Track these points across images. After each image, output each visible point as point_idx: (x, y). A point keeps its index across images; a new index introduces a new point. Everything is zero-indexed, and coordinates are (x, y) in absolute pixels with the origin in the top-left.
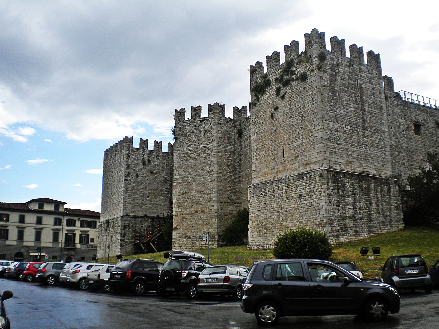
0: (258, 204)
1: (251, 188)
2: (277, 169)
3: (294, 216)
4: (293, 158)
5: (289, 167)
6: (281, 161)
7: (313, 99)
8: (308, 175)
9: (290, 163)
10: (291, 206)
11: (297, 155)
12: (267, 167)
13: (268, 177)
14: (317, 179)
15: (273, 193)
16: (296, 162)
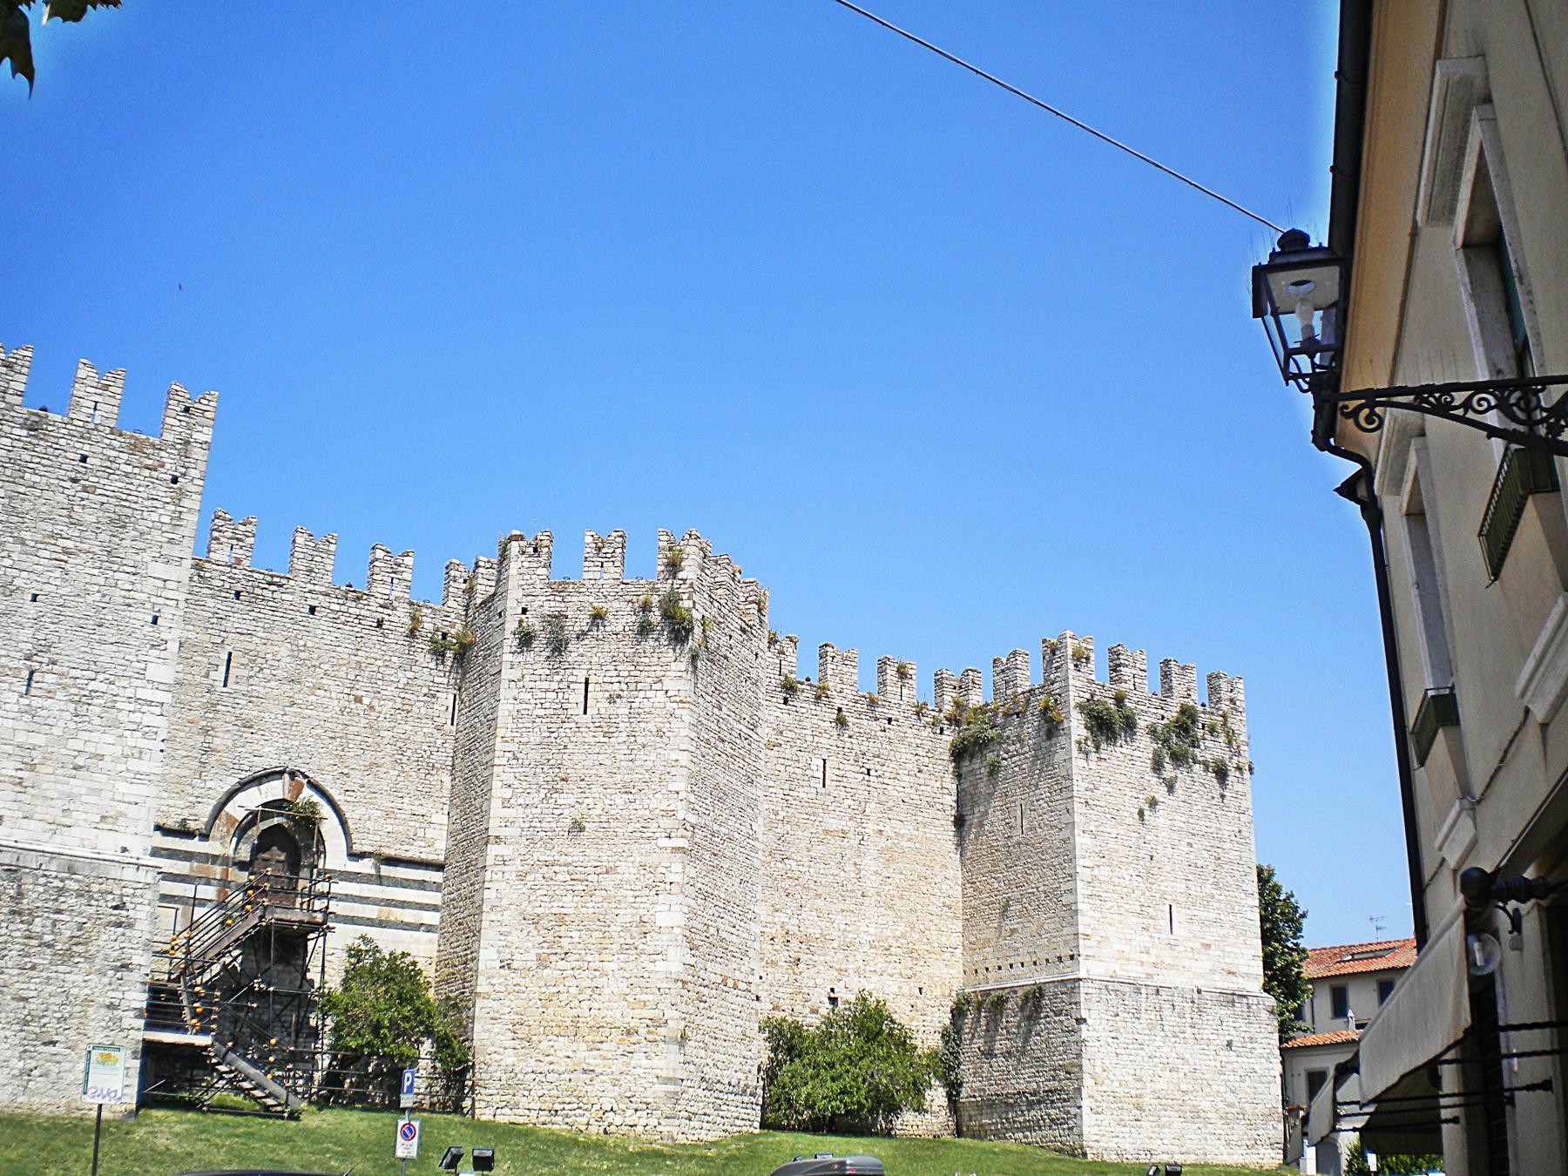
0: (1114, 1035)
1: (1090, 984)
2: (1157, 957)
3: (1215, 1088)
4: (1198, 946)
5: (1187, 963)
6: (1167, 942)
7: (1240, 831)
8: (1245, 1000)
9: (1190, 955)
10: (1207, 1063)
11: (1207, 942)
12: (1126, 939)
13: (1129, 967)
14: (1265, 1015)
15: (1158, 1018)
16: (1204, 957)
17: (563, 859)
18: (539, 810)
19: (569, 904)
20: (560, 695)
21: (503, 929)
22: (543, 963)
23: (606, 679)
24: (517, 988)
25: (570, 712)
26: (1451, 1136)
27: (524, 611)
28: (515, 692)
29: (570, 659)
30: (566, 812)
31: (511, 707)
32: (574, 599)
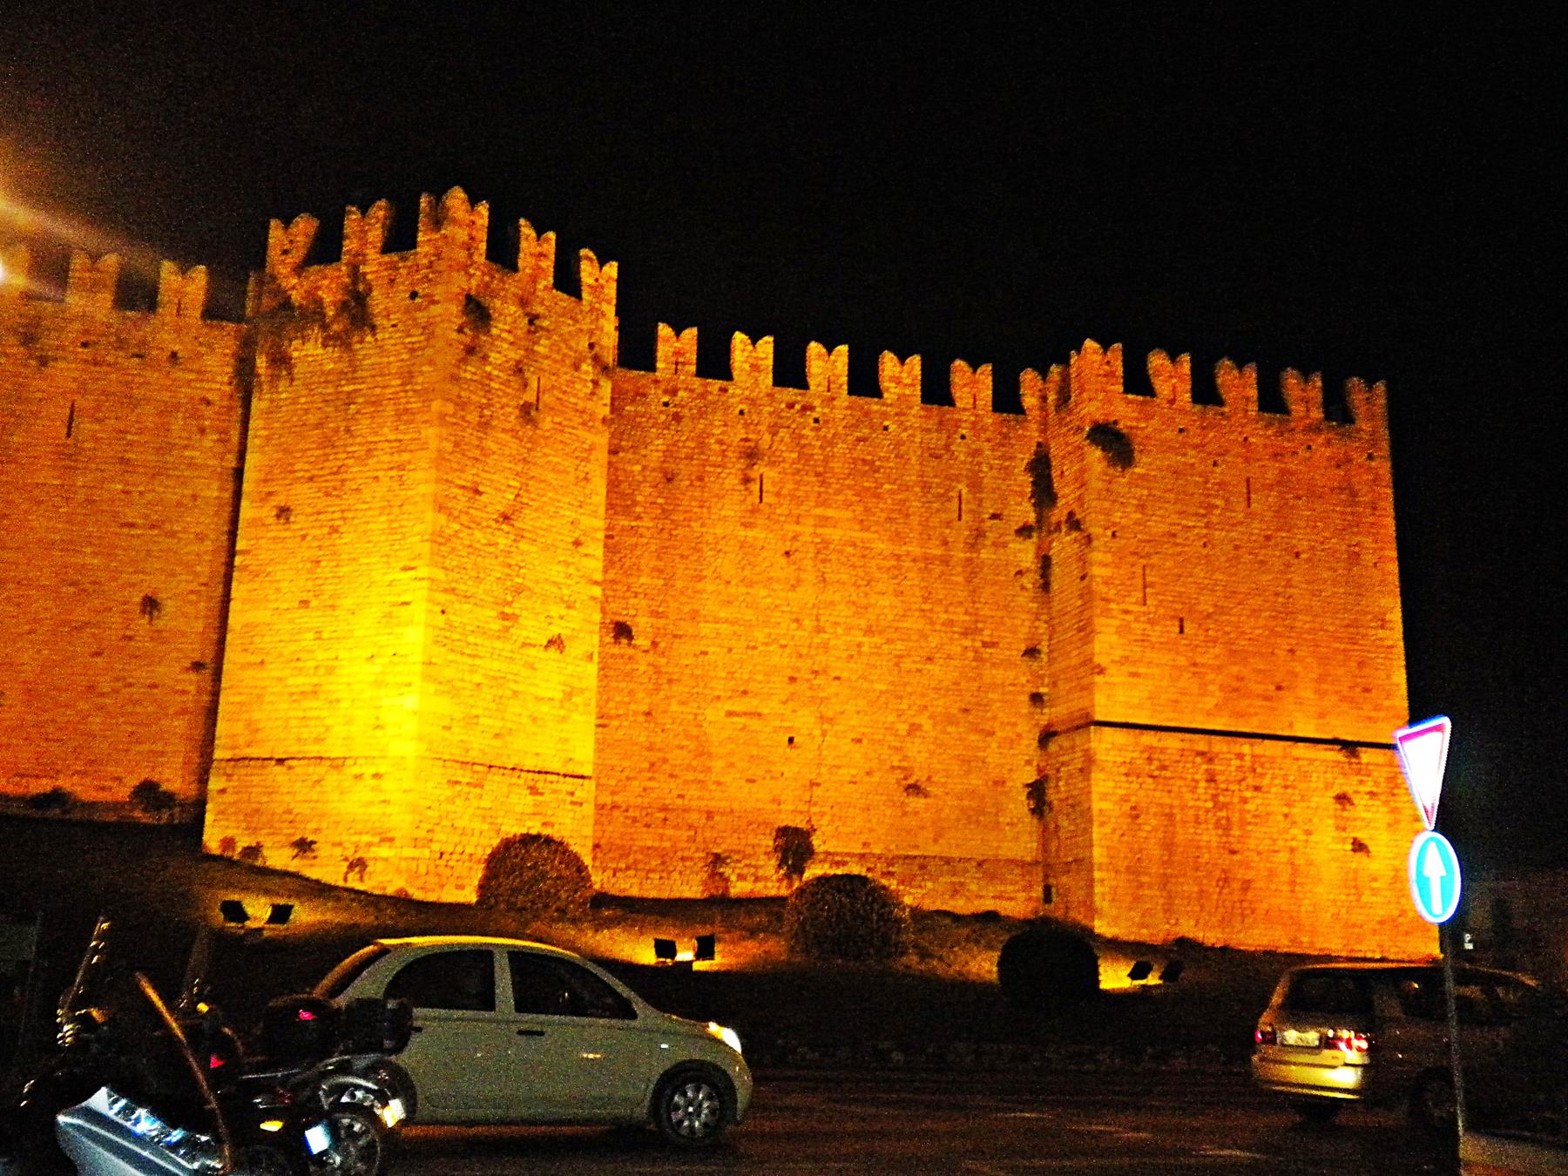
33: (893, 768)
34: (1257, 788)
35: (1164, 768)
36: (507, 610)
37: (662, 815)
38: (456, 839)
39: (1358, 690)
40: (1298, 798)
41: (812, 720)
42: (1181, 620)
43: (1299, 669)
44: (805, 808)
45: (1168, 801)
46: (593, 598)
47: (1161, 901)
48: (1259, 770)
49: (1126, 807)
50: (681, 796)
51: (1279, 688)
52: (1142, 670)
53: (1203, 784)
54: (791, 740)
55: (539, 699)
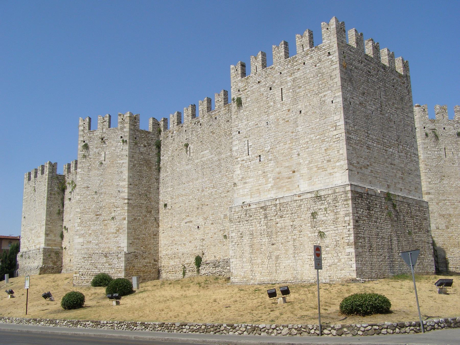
17: (447, 199)
18: (439, 185)
19: (451, 211)
20: (439, 152)
21: (435, 218)
22: (447, 227)
23: (450, 148)
24: (441, 235)
25: (442, 157)
26: (450, 278)
27: (424, 128)
28: (426, 151)
29: (439, 142)
30: (446, 185)
31: (426, 156)
32: (437, 125)
33: (221, 230)
34: (281, 217)
35: (251, 216)
36: (98, 213)
37: (174, 256)
38: (86, 271)
39: (325, 162)
40: (296, 217)
41: (202, 220)
42: (260, 156)
43: (301, 161)
44: (201, 248)
45: (252, 229)
46: (125, 203)
47: (250, 267)
48: (282, 209)
49: (239, 234)
50: (178, 249)
51: (294, 172)
52: (247, 181)
53: (263, 220)
54: (198, 227)
55: (108, 234)
